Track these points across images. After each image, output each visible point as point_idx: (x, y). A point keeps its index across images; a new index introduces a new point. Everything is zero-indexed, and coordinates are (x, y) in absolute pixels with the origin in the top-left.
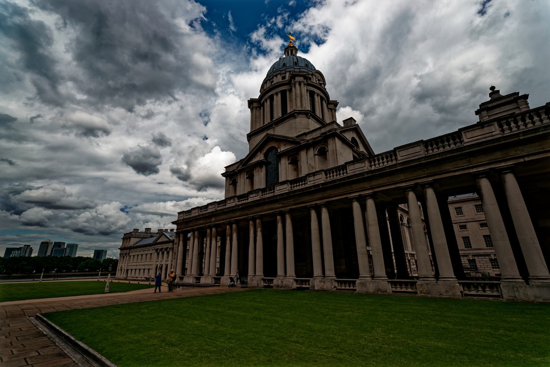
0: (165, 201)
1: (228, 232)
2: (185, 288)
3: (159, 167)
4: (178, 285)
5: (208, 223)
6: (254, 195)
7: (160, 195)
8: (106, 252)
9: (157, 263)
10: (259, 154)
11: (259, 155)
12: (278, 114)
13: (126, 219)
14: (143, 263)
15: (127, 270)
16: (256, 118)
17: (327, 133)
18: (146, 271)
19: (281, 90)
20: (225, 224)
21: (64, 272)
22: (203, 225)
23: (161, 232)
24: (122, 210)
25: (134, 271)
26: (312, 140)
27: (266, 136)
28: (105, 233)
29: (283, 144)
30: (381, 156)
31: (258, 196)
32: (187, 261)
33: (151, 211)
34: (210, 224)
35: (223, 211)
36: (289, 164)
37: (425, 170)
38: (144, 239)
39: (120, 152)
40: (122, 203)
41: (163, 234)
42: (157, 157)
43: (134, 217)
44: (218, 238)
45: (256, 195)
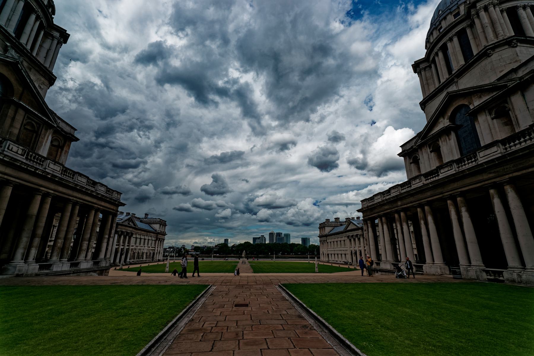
0: (347, 192)
1: (420, 214)
2: (384, 273)
3: (337, 162)
4: (377, 271)
5: (394, 208)
6: (446, 169)
7: (342, 187)
8: (309, 239)
9: (351, 249)
10: (441, 119)
11: (442, 121)
12: (458, 62)
13: (319, 211)
14: (339, 249)
15: (328, 254)
16: (427, 81)
18: (343, 256)
20: (415, 207)
21: (286, 255)
22: (389, 211)
23: (349, 221)
24: (315, 204)
25: (333, 255)
28: (307, 224)
31: (452, 169)
32: (380, 247)
33: (337, 202)
34: (396, 208)
35: (409, 193)
36: (493, 119)
38: (336, 228)
39: (305, 157)
40: (314, 198)
41: (351, 222)
42: (335, 153)
43: (324, 209)
44: (409, 222)
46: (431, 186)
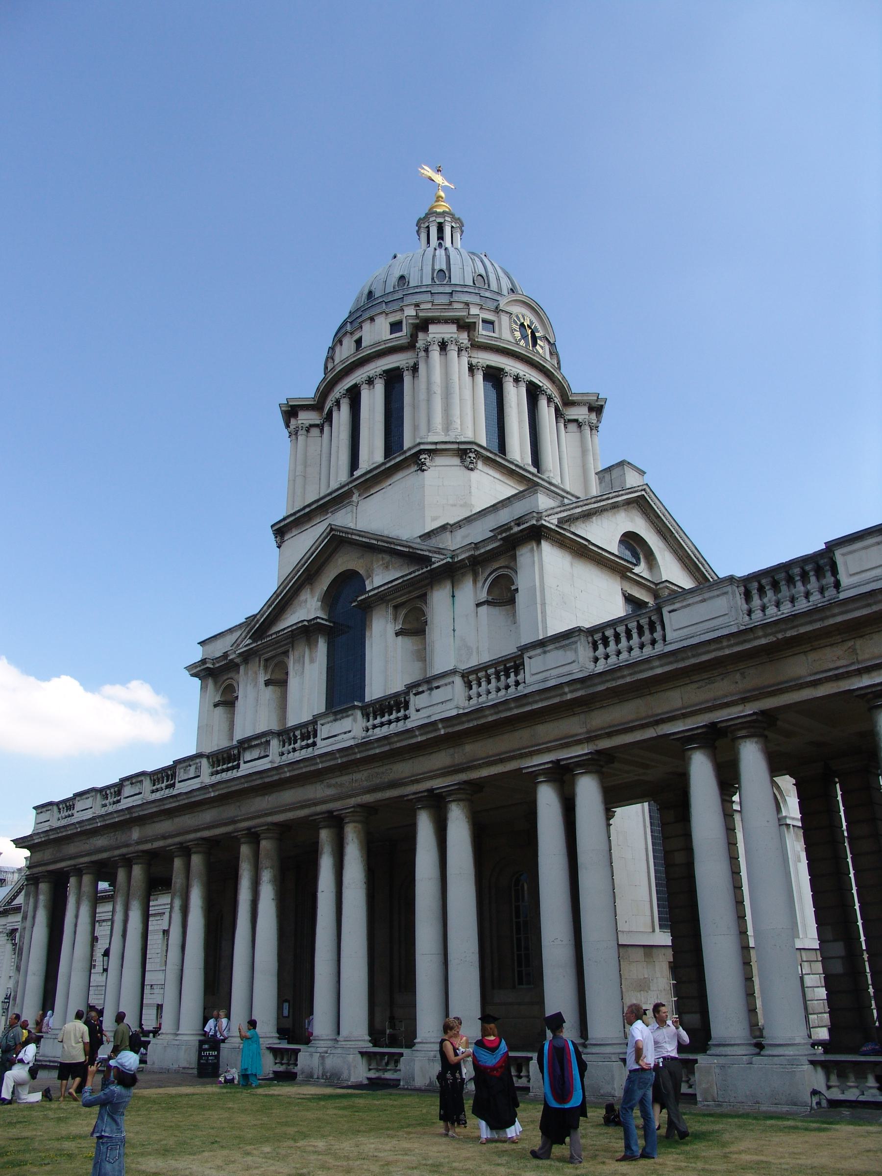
5: (118, 848)
6: (255, 753)
11: (306, 601)
12: (371, 453)
16: (305, 467)
17: (511, 528)
19: (384, 371)
26: (469, 550)
27: (328, 534)
29: (381, 562)
30: (624, 627)
31: (267, 756)
35: (162, 808)
36: (397, 634)
37: (738, 676)
45: (262, 754)
46: (212, 795)
